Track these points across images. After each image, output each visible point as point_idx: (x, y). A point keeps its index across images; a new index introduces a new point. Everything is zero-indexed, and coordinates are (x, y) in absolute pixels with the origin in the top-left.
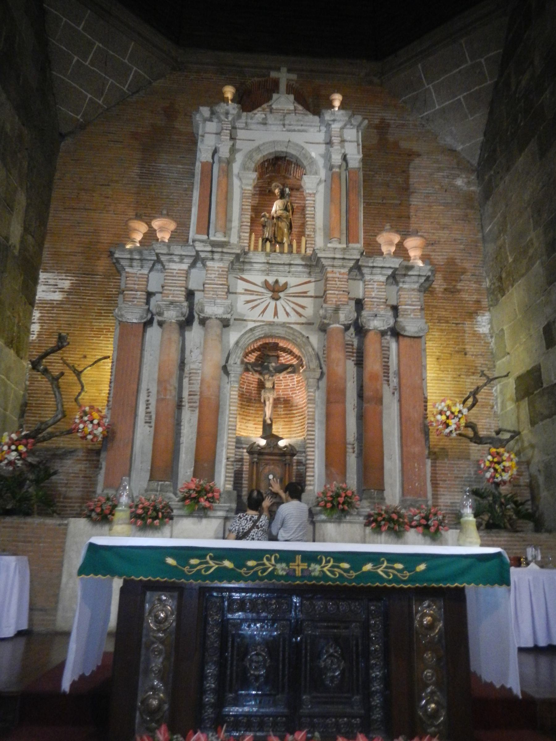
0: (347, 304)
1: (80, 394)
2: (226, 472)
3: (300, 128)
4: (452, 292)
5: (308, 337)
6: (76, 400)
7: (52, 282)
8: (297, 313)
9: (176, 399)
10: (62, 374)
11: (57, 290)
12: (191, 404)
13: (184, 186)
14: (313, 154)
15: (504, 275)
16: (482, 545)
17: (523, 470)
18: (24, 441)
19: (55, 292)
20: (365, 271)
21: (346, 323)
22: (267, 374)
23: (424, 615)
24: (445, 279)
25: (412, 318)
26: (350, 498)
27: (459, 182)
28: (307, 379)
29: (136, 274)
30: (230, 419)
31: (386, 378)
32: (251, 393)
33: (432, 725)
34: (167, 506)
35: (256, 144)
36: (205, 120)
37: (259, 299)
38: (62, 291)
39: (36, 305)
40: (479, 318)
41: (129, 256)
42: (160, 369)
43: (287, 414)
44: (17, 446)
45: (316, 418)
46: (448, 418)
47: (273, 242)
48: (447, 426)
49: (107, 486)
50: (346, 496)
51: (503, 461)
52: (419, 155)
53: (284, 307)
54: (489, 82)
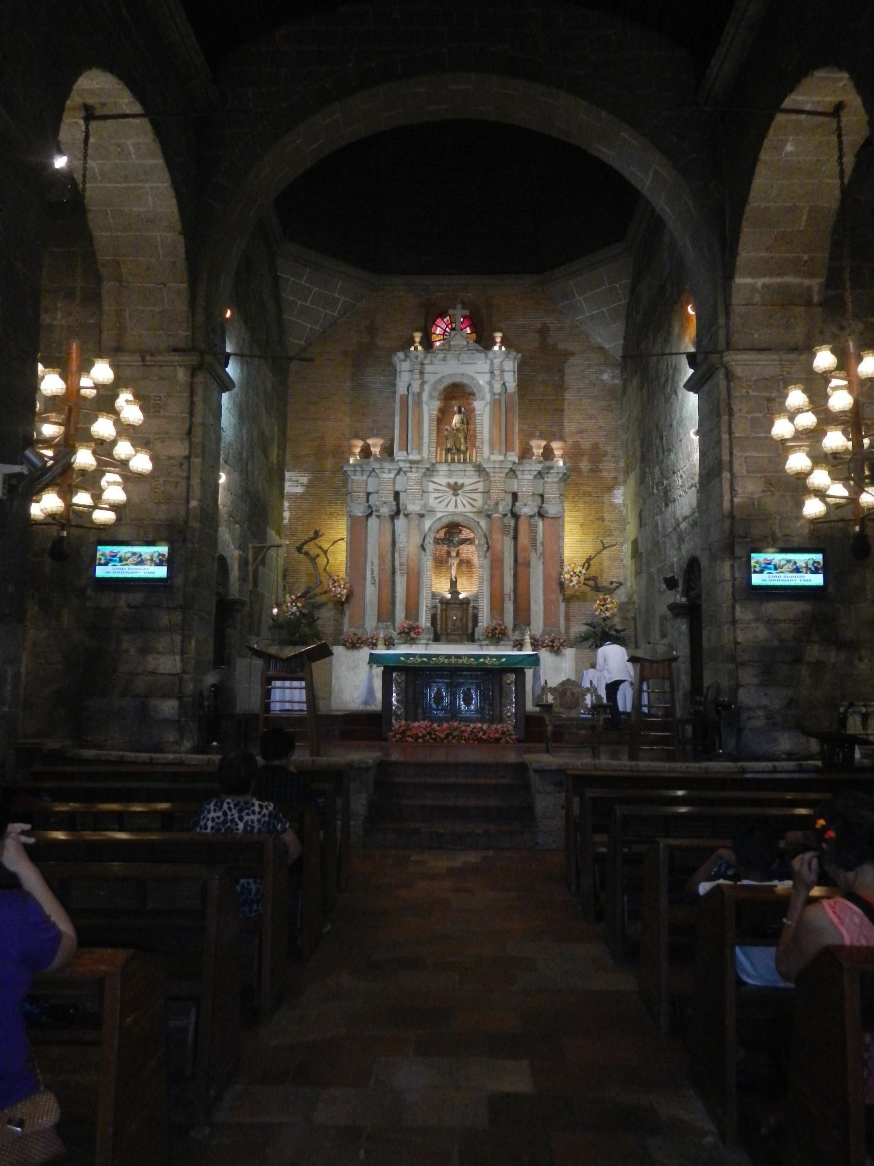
1: (326, 566)
2: (426, 615)
3: (471, 361)
4: (595, 471)
5: (478, 522)
6: (325, 569)
7: (294, 478)
10: (318, 555)
11: (299, 485)
12: (401, 572)
13: (386, 395)
14: (481, 382)
15: (629, 463)
16: (533, 651)
17: (630, 608)
18: (299, 600)
19: (297, 486)
20: (518, 473)
21: (503, 513)
23: (508, 679)
24: (590, 460)
25: (553, 504)
26: (504, 630)
27: (605, 377)
28: (478, 551)
32: (442, 557)
33: (509, 721)
34: (391, 638)
35: (438, 377)
36: (402, 361)
38: (302, 485)
39: (285, 497)
40: (615, 492)
41: (352, 469)
42: (379, 548)
43: (468, 571)
44: (296, 604)
45: (485, 578)
46: (571, 576)
47: (454, 451)
48: (572, 581)
49: (351, 626)
50: (501, 629)
51: (607, 604)
52: (572, 354)
53: (461, 501)
54: (624, 302)
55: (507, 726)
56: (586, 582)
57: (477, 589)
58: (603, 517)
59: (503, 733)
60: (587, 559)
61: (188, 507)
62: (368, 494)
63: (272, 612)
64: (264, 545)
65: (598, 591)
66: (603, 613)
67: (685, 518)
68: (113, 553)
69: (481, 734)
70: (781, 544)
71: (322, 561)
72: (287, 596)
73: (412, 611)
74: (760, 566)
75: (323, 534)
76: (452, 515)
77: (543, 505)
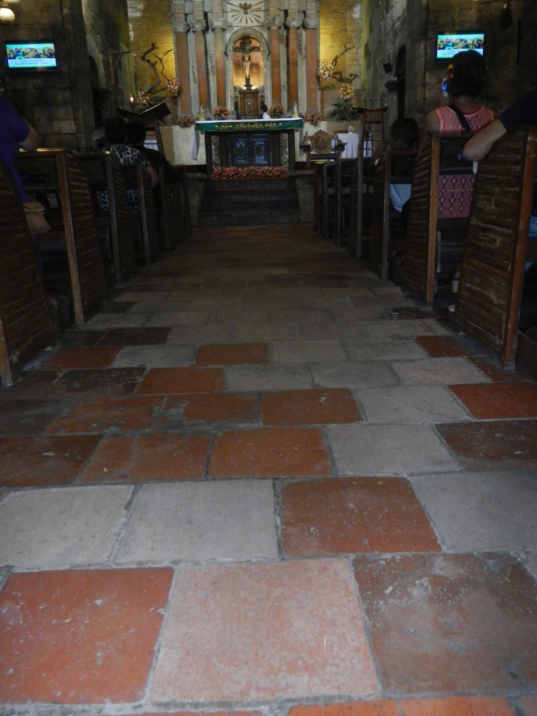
0: (279, 16)
1: (163, 70)
2: (231, 103)
5: (262, 34)
6: (162, 73)
7: (134, 6)
8: (257, 20)
9: (206, 70)
10: (156, 62)
11: (138, 10)
12: (213, 72)
16: (299, 118)
18: (147, 95)
19: (137, 12)
21: (279, 25)
22: (245, 53)
23: (283, 137)
25: (312, 18)
29: (178, 4)
30: (231, 78)
31: (300, 52)
32: (240, 62)
33: (285, 164)
37: (238, 14)
39: (129, 21)
40: (355, 9)
42: (197, 56)
45: (268, 75)
46: (325, 71)
48: (325, 74)
49: (183, 112)
50: (279, 110)
51: (347, 90)
55: (284, 168)
56: (334, 76)
57: (262, 85)
58: (346, 28)
59: (282, 172)
60: (335, 58)
61: (62, 14)
62: (186, 15)
63: (130, 101)
64: (119, 52)
65: (342, 82)
66: (345, 97)
67: (399, 18)
68: (17, 49)
69: (268, 172)
70: (457, 28)
71: (159, 67)
72: (139, 92)
73: (221, 100)
74: (443, 44)
75: (158, 48)
76: (244, 28)
77: (306, 20)
